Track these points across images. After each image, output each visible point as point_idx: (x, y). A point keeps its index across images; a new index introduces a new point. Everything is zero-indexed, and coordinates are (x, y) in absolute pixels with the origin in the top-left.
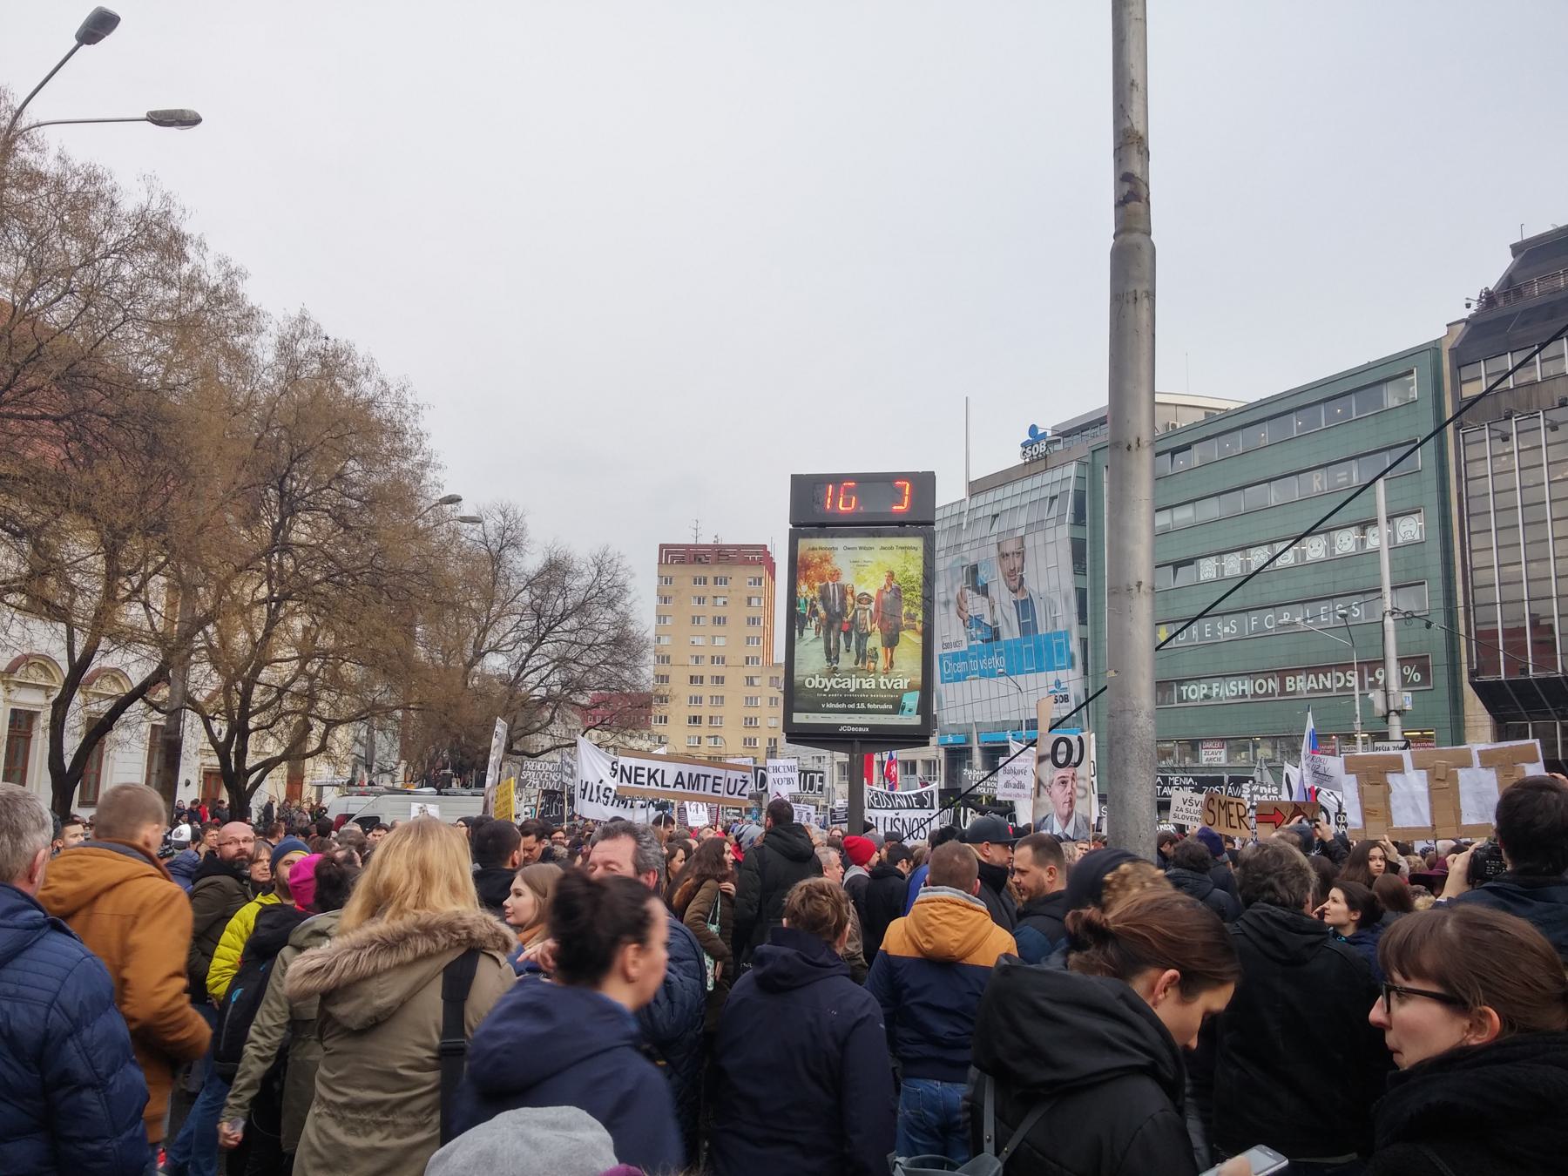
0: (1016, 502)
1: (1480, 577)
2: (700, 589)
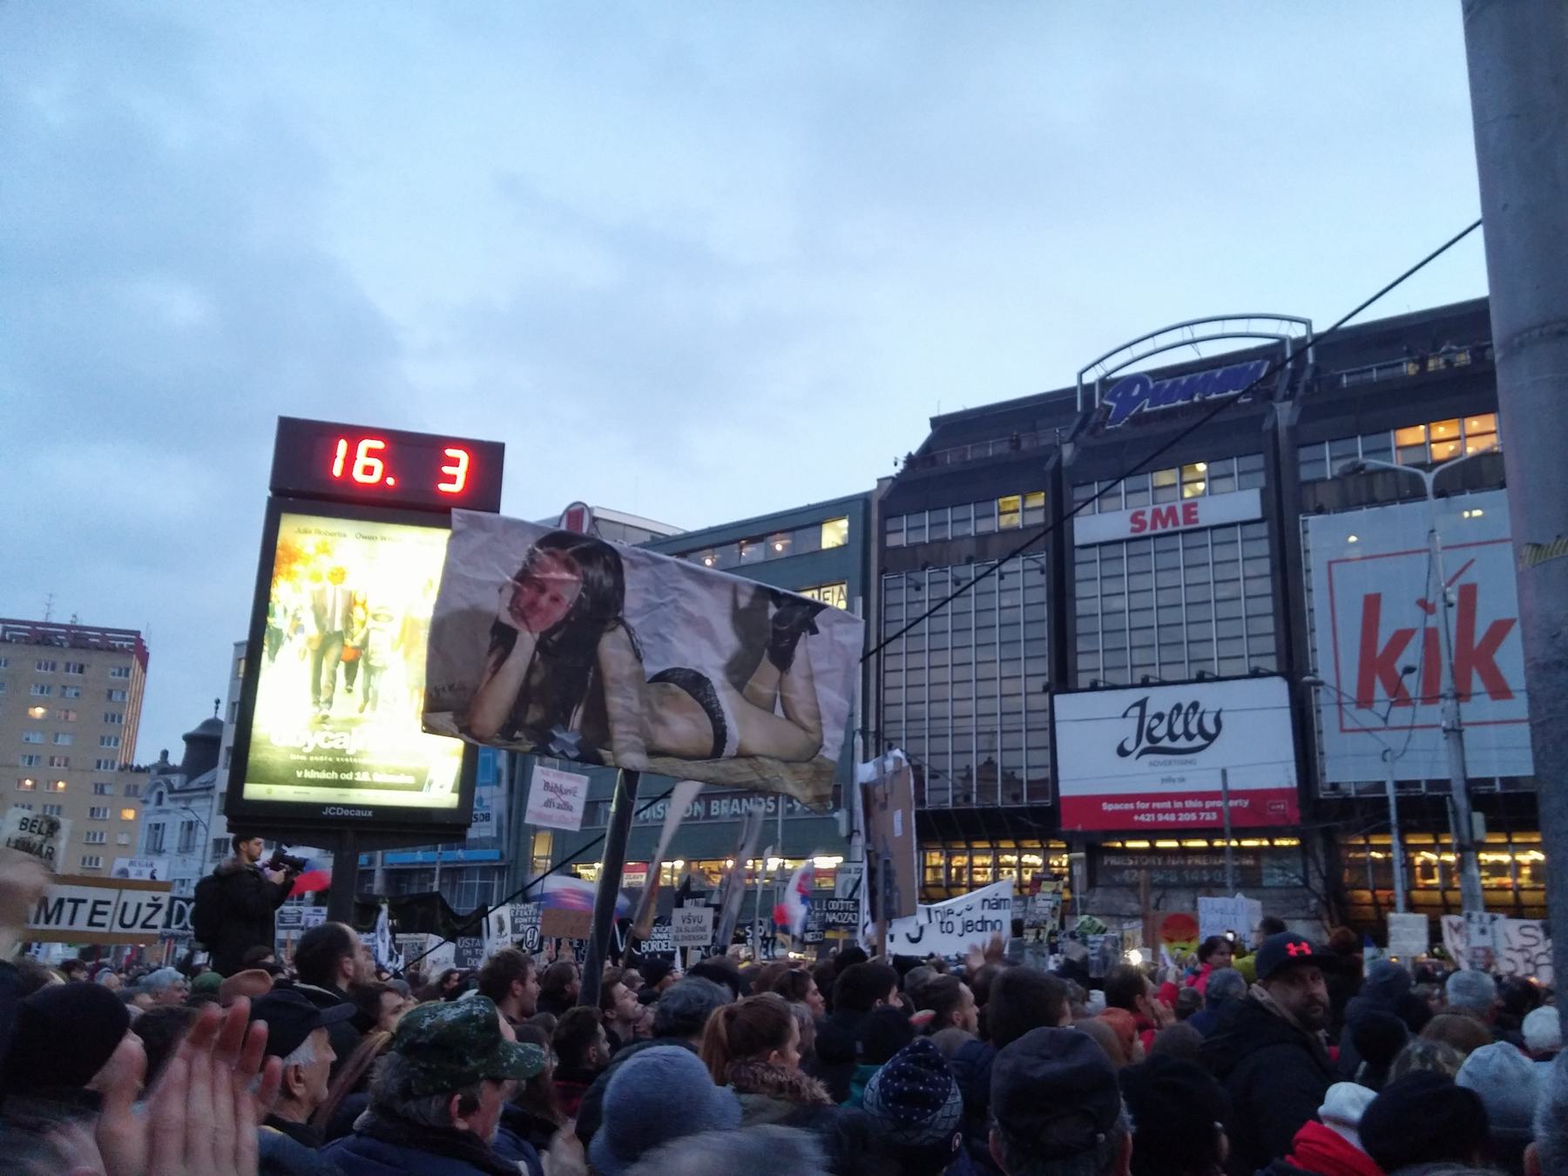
1: (890, 713)
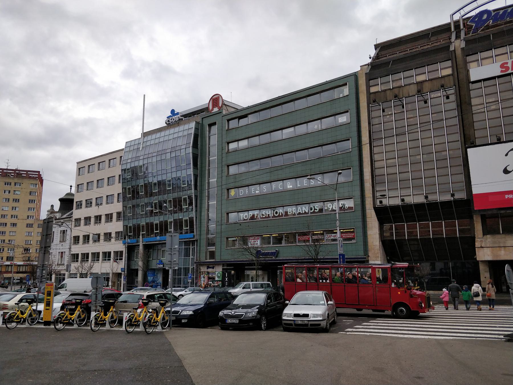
0: (166, 138)
1: (377, 165)
2: (8, 188)
